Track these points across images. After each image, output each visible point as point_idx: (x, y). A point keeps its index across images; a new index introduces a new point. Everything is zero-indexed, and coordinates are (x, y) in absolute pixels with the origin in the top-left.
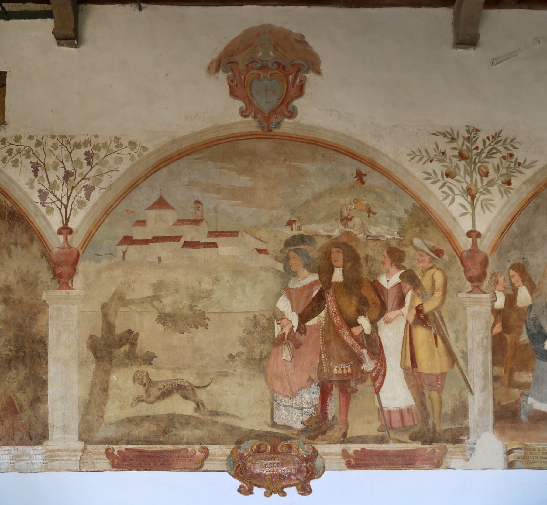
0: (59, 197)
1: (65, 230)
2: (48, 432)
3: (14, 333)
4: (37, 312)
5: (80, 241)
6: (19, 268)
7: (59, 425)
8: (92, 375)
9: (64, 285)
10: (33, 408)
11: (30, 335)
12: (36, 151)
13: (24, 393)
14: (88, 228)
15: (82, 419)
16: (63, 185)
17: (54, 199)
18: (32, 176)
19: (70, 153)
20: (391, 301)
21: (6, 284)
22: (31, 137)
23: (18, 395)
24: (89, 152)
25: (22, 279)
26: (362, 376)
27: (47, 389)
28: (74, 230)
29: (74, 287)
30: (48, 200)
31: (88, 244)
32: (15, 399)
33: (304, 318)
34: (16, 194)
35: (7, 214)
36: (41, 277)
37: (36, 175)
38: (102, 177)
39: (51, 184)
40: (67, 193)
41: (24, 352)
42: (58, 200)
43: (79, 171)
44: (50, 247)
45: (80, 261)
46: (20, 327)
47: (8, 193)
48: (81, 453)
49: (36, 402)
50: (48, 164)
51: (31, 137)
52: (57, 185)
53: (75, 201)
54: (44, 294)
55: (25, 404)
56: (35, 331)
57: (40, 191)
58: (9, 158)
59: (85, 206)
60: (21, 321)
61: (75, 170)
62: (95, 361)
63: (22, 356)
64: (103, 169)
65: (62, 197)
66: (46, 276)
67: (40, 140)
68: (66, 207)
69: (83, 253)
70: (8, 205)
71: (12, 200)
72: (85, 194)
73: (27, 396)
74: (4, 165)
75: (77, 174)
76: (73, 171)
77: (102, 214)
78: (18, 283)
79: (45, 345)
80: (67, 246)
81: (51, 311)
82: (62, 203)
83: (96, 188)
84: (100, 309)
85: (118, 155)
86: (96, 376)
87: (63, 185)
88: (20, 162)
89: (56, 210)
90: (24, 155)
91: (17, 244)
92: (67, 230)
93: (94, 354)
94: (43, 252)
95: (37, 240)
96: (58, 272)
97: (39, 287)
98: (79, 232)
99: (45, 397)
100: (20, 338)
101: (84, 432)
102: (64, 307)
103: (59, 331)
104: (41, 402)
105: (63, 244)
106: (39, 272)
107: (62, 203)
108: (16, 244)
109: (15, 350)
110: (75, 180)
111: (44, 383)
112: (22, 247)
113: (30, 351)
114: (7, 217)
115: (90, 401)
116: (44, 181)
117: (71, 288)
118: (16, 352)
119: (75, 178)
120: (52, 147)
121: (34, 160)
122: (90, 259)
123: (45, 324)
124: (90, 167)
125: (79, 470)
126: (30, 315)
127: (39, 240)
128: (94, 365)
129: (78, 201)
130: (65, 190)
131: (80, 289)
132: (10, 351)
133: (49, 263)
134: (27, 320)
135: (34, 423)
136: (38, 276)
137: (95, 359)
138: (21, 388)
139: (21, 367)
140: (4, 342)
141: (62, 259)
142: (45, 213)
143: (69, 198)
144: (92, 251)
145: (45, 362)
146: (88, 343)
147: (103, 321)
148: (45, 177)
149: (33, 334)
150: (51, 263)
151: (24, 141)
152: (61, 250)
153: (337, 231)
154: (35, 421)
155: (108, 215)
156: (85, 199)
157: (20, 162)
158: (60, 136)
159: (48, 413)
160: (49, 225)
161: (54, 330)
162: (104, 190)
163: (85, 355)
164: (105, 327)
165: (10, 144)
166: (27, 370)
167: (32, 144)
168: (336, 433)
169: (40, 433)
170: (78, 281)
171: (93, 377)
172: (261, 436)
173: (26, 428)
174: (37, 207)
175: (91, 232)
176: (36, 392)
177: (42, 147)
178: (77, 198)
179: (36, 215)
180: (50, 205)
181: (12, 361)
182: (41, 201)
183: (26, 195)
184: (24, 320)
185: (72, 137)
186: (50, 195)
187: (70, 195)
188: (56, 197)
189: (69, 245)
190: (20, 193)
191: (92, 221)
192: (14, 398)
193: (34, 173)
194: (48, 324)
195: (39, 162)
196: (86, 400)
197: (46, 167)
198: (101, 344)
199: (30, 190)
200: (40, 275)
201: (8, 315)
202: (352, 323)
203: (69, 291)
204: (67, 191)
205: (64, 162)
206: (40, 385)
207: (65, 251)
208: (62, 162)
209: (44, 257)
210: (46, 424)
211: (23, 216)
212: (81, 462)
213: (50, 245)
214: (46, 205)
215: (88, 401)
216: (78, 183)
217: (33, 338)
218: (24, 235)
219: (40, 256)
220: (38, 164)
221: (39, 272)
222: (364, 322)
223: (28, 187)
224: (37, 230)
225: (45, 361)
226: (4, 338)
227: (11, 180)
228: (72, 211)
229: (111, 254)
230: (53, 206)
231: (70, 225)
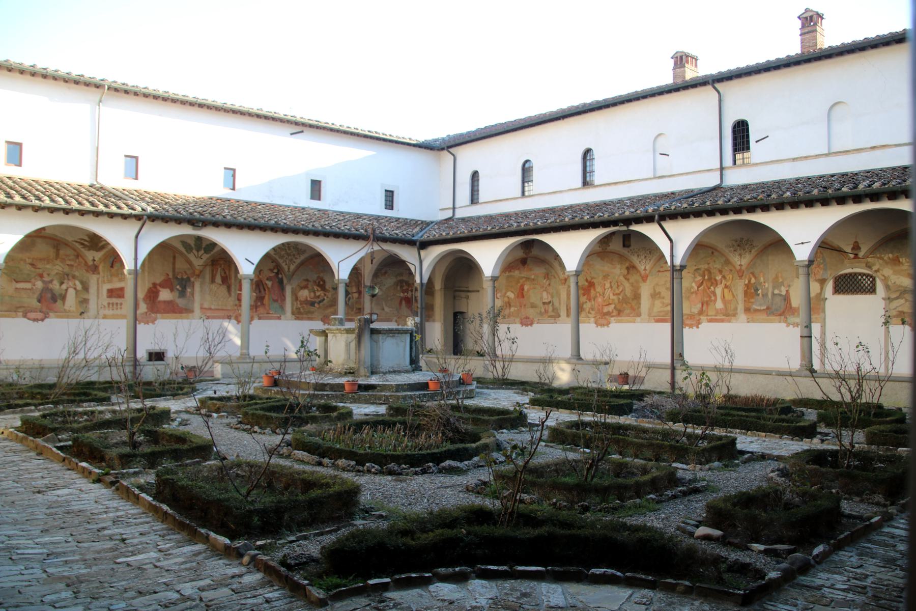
20: (719, 283)
26: (711, 301)
33: (698, 287)
153: (706, 266)
168: (705, 314)
172: (688, 315)
202: (709, 288)
222: (712, 288)
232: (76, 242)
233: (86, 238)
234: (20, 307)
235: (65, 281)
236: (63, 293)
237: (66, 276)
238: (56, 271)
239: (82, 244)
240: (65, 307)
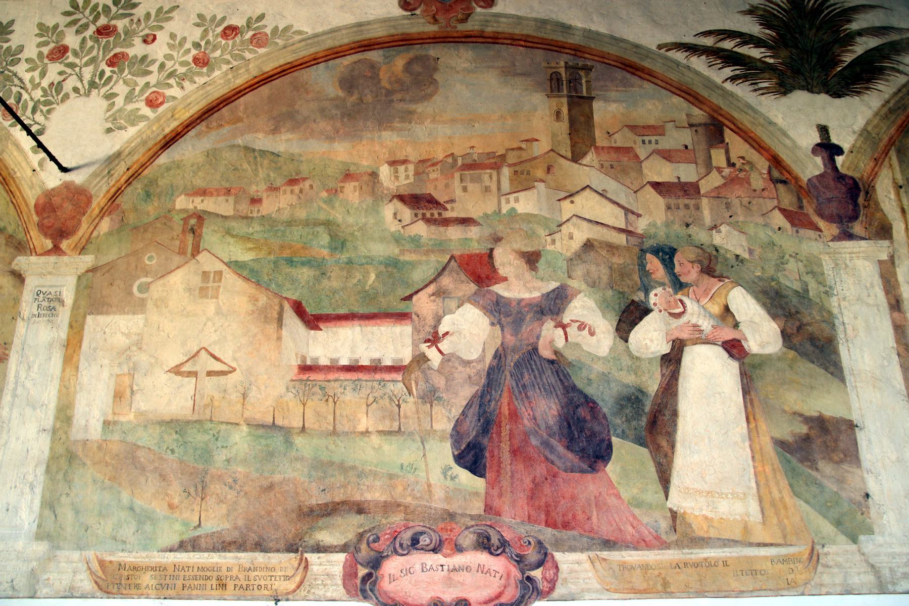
232: (692, 49)
233: (752, 27)
234: (331, 510)
235: (656, 297)
236: (653, 384)
237: (654, 264)
238: (581, 234)
239: (730, 58)
240: (676, 500)
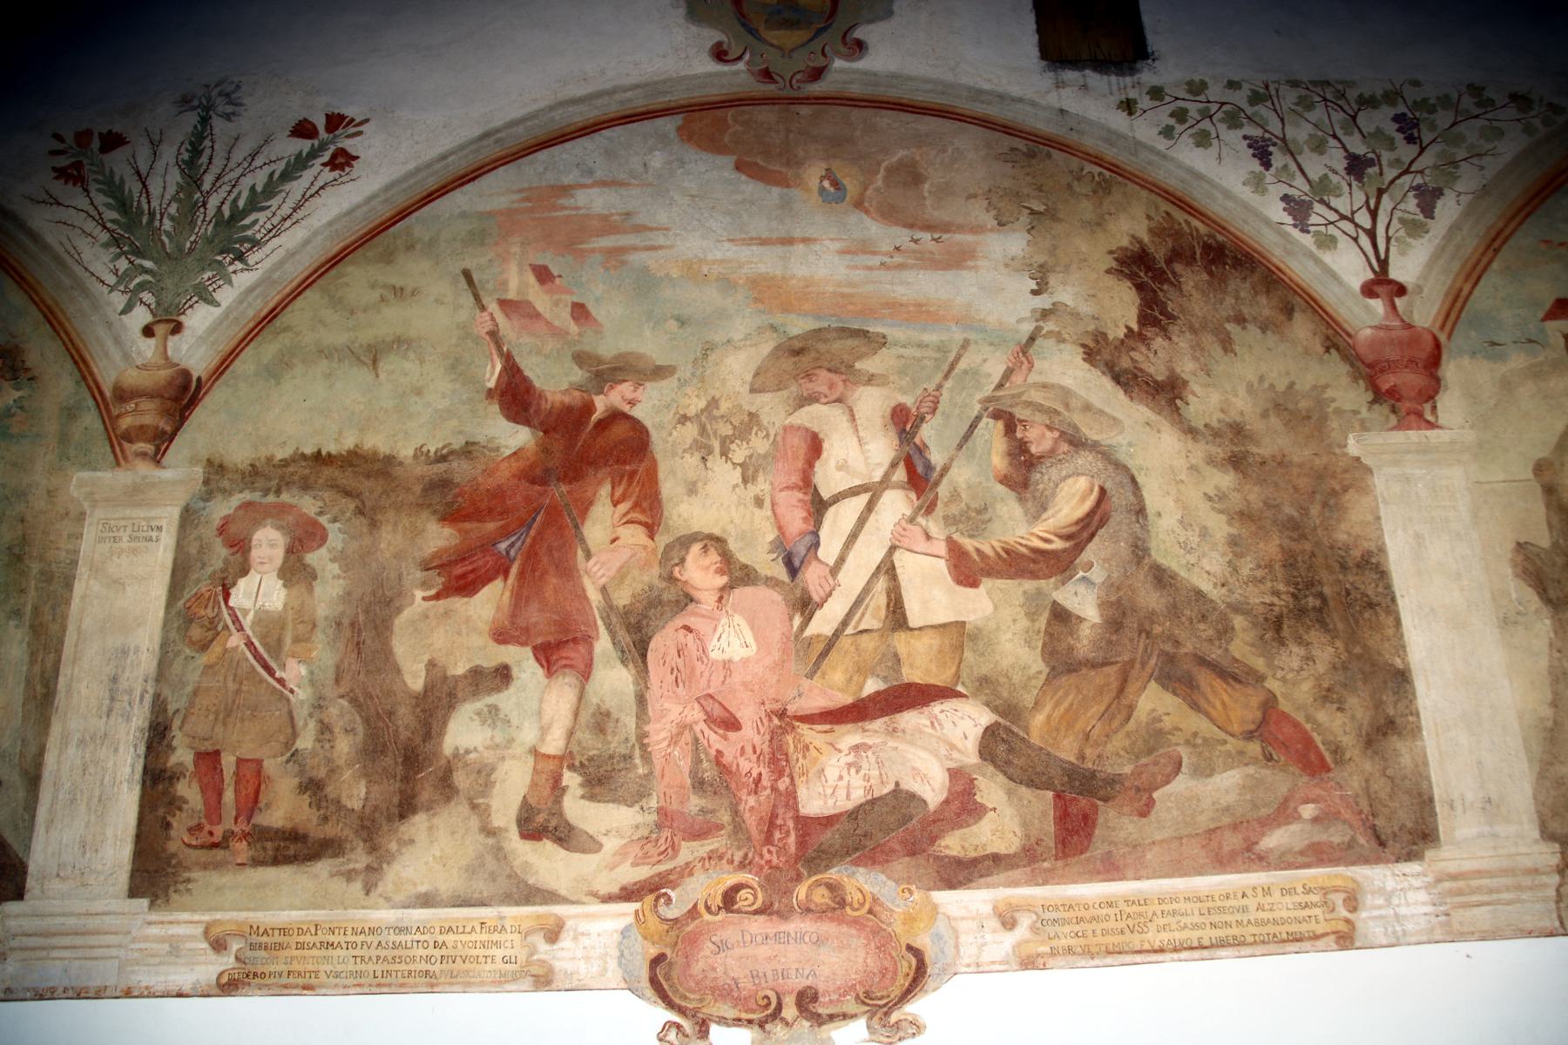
0: (1346, 211)
1: (1381, 284)
2: (1436, 821)
3: (1281, 546)
4: (1337, 487)
5: (1434, 311)
6: (1261, 379)
7: (1470, 796)
8: (1546, 650)
9: (1413, 417)
10: (1376, 753)
11: (1332, 547)
12: (1255, 114)
13: (1339, 709)
14: (1449, 282)
15: (1542, 776)
16: (1350, 185)
17: (1333, 217)
18: (1256, 166)
19: (1354, 118)
21: (1228, 420)
22: (1233, 85)
23: (1322, 716)
24: (1404, 115)
25: (1277, 406)
27: (1414, 694)
28: (1410, 288)
29: (1441, 422)
30: (1314, 219)
31: (1458, 317)
32: (1313, 730)
34: (1217, 207)
35: (1198, 251)
36: (1333, 400)
37: (1267, 165)
38: (1456, 168)
39: (1314, 184)
40: (1367, 202)
41: (1321, 595)
42: (1343, 217)
43: (1386, 156)
44: (1346, 326)
45: (1444, 357)
46: (1295, 528)
47: (1195, 204)
48: (1556, 879)
49: (1385, 734)
50: (1295, 141)
51: (1233, 85)
52: (1332, 186)
53: (1395, 221)
54: (1351, 441)
55: (1348, 740)
56: (1341, 537)
57: (1285, 198)
58: (1179, 128)
59: (1427, 232)
60: (1295, 514)
61: (1374, 152)
62: (1546, 611)
63: (1314, 608)
64: (1453, 150)
65: (1353, 213)
66: (1349, 395)
67: (1262, 91)
68: (1372, 234)
69: (1449, 337)
70: (1197, 230)
71: (1209, 219)
72: (1418, 205)
73: (1353, 718)
74: (1171, 143)
75: (1384, 162)
76: (1370, 155)
77: (1481, 250)
78: (1265, 415)
79: (1383, 574)
80: (1397, 323)
81: (1380, 482)
82: (1357, 225)
83: (1446, 191)
84: (1531, 476)
85: (1487, 123)
86: (1559, 651)
87: (1350, 185)
88: (1214, 135)
89: (1344, 243)
90: (1222, 120)
91: (1245, 320)
92: (1390, 287)
93: (1538, 593)
94: (1328, 338)
95: (1303, 311)
96: (1385, 387)
97: (1334, 424)
98: (1426, 290)
99: (1411, 719)
100: (1300, 559)
101: (1555, 814)
102: (1418, 472)
103: (1418, 536)
104: (1400, 734)
105: (1386, 318)
106: (1327, 386)
107: (1357, 225)
108: (1241, 320)
109: (1292, 590)
110: (1381, 174)
111: (1401, 678)
112: (1261, 328)
113: (1339, 594)
114: (1202, 258)
115: (1556, 723)
116: (1293, 176)
117: (1432, 426)
118: (1293, 595)
119: (1381, 169)
120: (1297, 104)
121: (1256, 132)
122: (1474, 353)
123: (1370, 518)
124: (1415, 149)
125: (1561, 931)
126: (1318, 497)
127: (1310, 310)
128: (1548, 622)
129: (1402, 221)
130: (1359, 198)
131: (1463, 427)
132: (1276, 593)
133: (1352, 365)
134: (1315, 510)
135: (1383, 795)
136: (1325, 396)
137: (1546, 604)
138: (1326, 696)
139: (1315, 636)
140: (1251, 569)
141: (1391, 354)
142: (1313, 248)
143: (1374, 214)
144: (1473, 333)
145: (1390, 621)
146: (1515, 565)
147: (1548, 506)
148: (1293, 167)
149: (1340, 545)
150: (1359, 364)
151: (1215, 92)
152: (1382, 333)
154: (1388, 790)
155: (1496, 251)
156: (1421, 217)
157: (1214, 135)
158: (1315, 83)
159: (1426, 764)
160: (1334, 276)
161: (1400, 532)
162: (1471, 197)
163: (1514, 596)
164: (1555, 520)
165: (1177, 99)
166: (1339, 644)
167: (1240, 98)
169: (1409, 825)
170: (1450, 406)
171: (1550, 656)
173: (1361, 812)
174: (1286, 235)
175: (1461, 290)
176: (1378, 705)
177: (1269, 104)
178: (1398, 214)
179: (1289, 253)
180: (1322, 229)
181: (1286, 622)
182: (1294, 219)
183: (1246, 206)
184: (1304, 511)
185: (1351, 84)
186: (1318, 207)
187: (1377, 207)
188: (1336, 211)
189: (1403, 321)
190: (1230, 204)
191: (1456, 266)
192: (1308, 727)
193: (1260, 159)
194: (1379, 518)
195: (1267, 135)
196: (1542, 720)
197: (1291, 146)
198: (1554, 564)
199: (1256, 197)
200: (1329, 393)
201: (1252, 497)
203: (1428, 433)
204: (1364, 199)
205: (1340, 133)
206: (1390, 684)
207: (1394, 334)
208: (1335, 136)
209: (1332, 351)
210: (1426, 797)
211: (1247, 255)
212: (1562, 905)
213: (1346, 321)
214: (1311, 228)
215: (1549, 724)
216: (1392, 182)
217: (1342, 557)
218: (1263, 300)
219: (1320, 349)
220: (1263, 139)
221: (1327, 386)
223: (1247, 190)
224: (1298, 286)
225: (1392, 619)
226: (1249, 559)
227: (1199, 177)
228: (1393, 242)
229: (1530, 341)
230: (1332, 230)
231: (1394, 274)
